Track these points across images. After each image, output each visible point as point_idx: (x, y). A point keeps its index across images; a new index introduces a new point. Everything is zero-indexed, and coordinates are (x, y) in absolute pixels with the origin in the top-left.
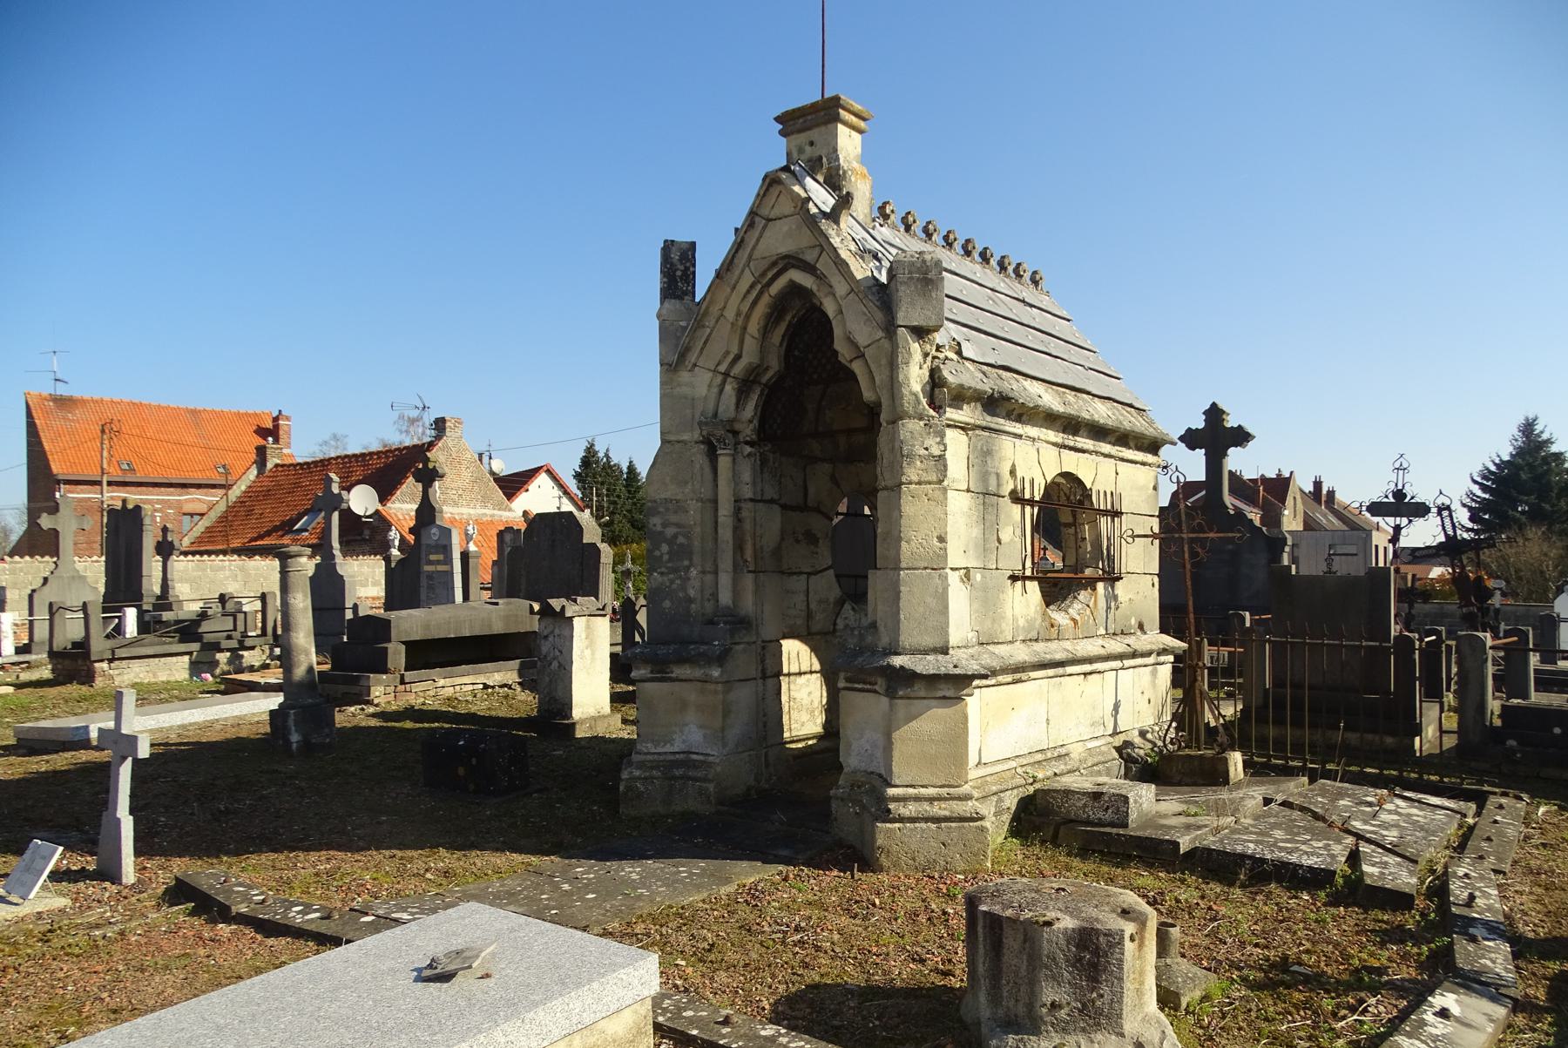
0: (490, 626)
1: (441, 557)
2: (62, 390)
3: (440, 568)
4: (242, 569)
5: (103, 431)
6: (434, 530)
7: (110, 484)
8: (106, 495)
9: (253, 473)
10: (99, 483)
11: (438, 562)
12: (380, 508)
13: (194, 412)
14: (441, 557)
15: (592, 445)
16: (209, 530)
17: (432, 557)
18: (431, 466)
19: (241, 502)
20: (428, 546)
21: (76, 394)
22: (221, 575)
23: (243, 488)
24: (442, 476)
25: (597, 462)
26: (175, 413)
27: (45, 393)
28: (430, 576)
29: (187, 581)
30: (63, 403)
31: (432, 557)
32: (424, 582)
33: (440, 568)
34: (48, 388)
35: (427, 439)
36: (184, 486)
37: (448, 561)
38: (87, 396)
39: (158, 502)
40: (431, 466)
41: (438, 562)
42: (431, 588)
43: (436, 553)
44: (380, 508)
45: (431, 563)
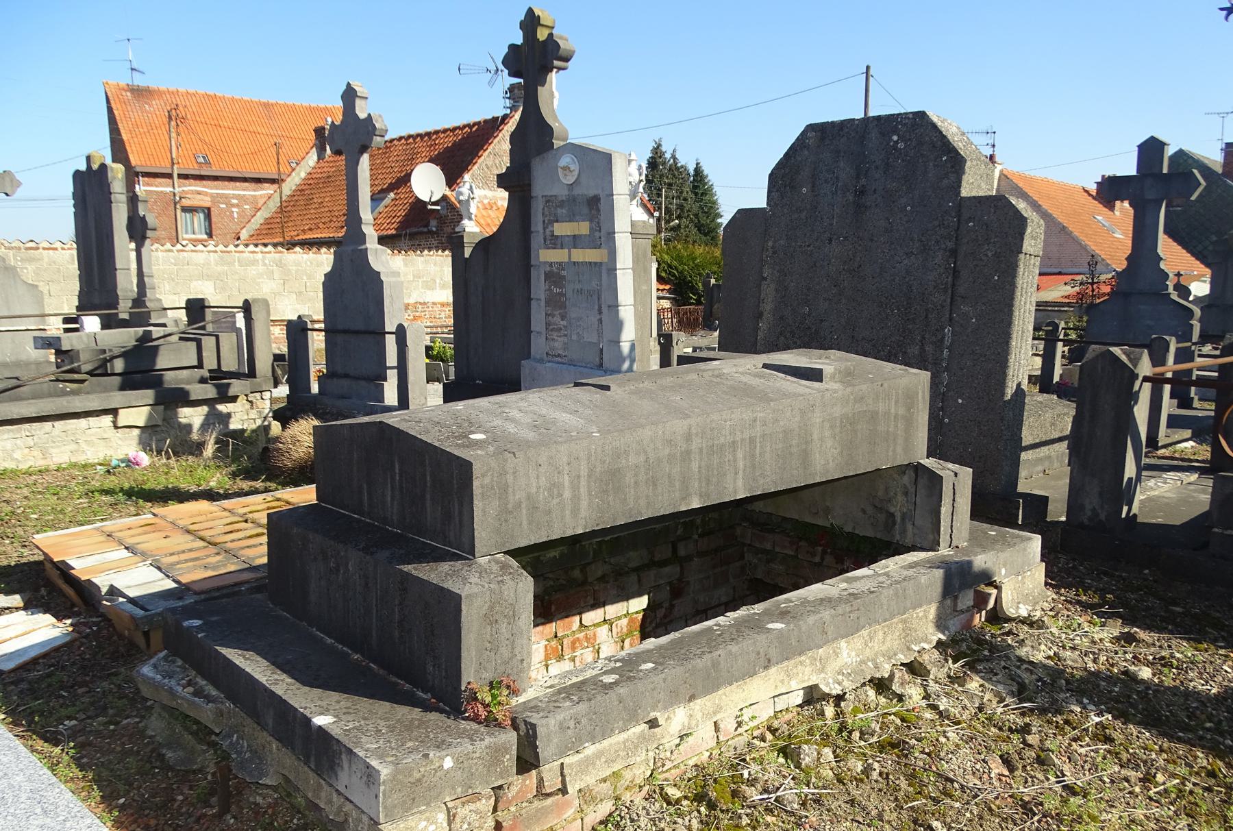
0: (805, 455)
1: (583, 228)
2: (139, 81)
3: (579, 255)
4: (280, 264)
5: (170, 118)
6: (566, 160)
7: (180, 176)
8: (177, 190)
9: (313, 157)
10: (170, 176)
11: (576, 241)
12: (448, 193)
13: (266, 105)
14: (583, 228)
15: (659, 146)
16: (268, 222)
17: (561, 229)
18: (542, 35)
19: (300, 191)
20: (548, 200)
21: (153, 85)
22: (252, 271)
23: (303, 175)
24: (567, 60)
25: (664, 163)
26: (248, 106)
27: (123, 83)
28: (554, 276)
29: (208, 277)
30: (141, 93)
31: (561, 229)
32: (539, 289)
33: (579, 255)
34: (125, 79)
35: (500, 113)
36: (258, 181)
37: (603, 236)
38: (163, 88)
39: (235, 197)
40: (542, 35)
41: (576, 241)
42: (556, 303)
43: (571, 218)
44: (448, 193)
45: (555, 242)
